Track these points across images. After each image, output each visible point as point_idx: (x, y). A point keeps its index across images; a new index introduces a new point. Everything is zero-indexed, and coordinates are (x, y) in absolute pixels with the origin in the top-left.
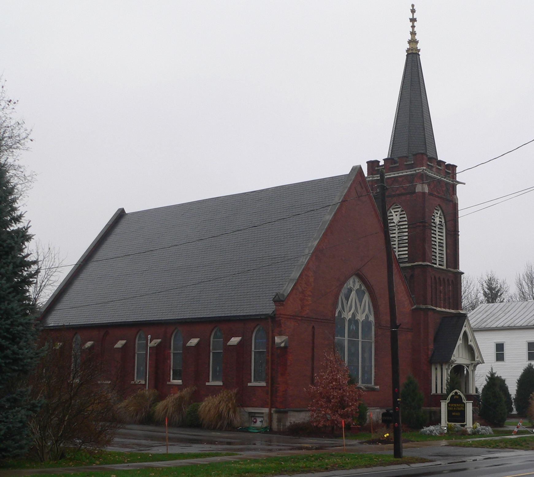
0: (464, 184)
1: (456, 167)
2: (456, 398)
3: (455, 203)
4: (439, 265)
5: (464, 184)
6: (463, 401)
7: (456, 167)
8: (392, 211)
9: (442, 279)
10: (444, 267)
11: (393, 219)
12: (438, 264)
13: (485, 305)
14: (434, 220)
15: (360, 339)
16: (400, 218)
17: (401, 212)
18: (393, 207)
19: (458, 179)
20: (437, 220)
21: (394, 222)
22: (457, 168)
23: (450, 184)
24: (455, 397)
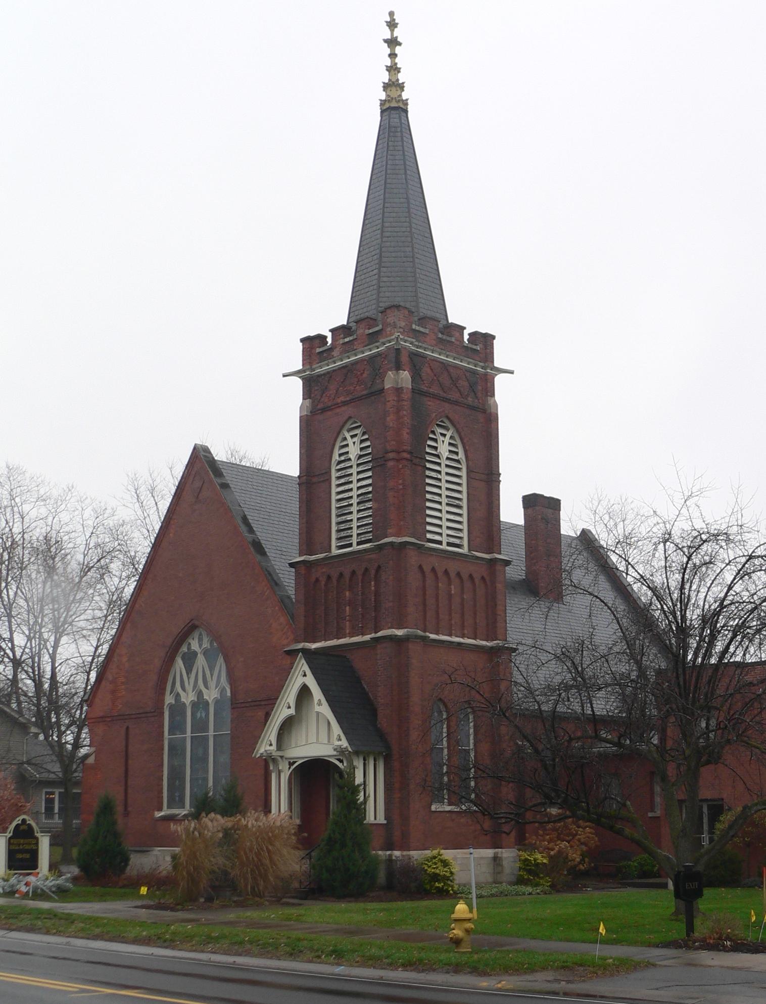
0: (512, 372)
1: (493, 337)
2: (23, 830)
3: (491, 413)
4: (449, 544)
5: (512, 372)
6: (36, 834)
7: (493, 337)
8: (348, 436)
9: (440, 574)
10: (465, 550)
11: (347, 453)
12: (444, 543)
13: (318, 576)
14: (436, 448)
15: (211, 733)
16: (362, 449)
17: (362, 436)
18: (348, 426)
19: (497, 363)
20: (444, 449)
21: (350, 459)
22: (494, 341)
23: (426, 358)
24: (22, 827)
